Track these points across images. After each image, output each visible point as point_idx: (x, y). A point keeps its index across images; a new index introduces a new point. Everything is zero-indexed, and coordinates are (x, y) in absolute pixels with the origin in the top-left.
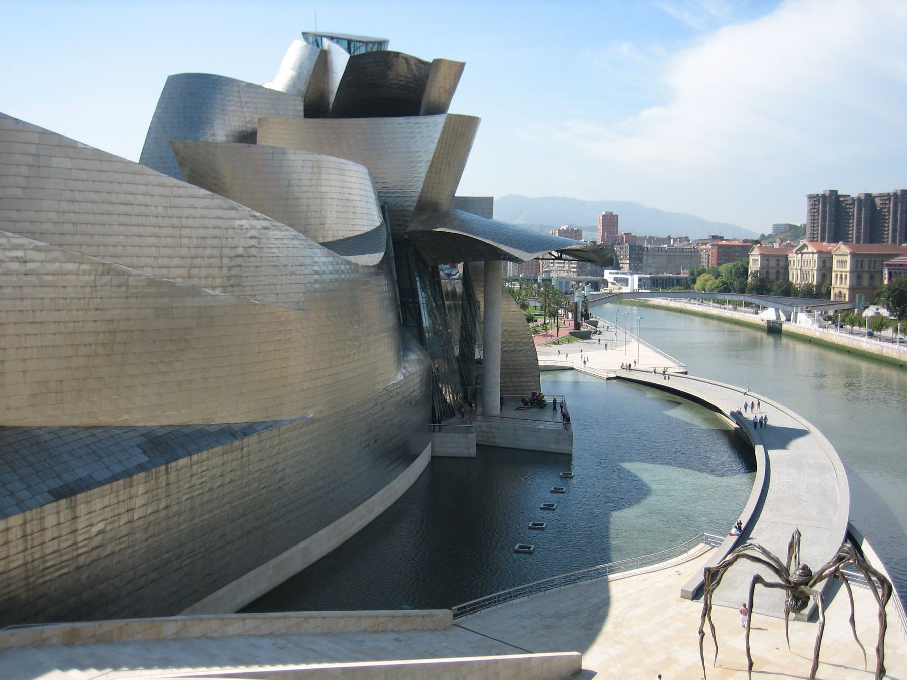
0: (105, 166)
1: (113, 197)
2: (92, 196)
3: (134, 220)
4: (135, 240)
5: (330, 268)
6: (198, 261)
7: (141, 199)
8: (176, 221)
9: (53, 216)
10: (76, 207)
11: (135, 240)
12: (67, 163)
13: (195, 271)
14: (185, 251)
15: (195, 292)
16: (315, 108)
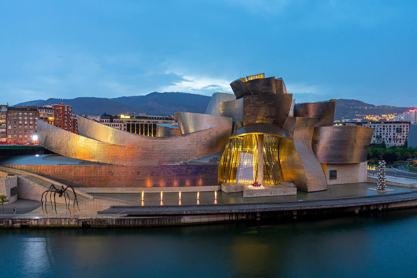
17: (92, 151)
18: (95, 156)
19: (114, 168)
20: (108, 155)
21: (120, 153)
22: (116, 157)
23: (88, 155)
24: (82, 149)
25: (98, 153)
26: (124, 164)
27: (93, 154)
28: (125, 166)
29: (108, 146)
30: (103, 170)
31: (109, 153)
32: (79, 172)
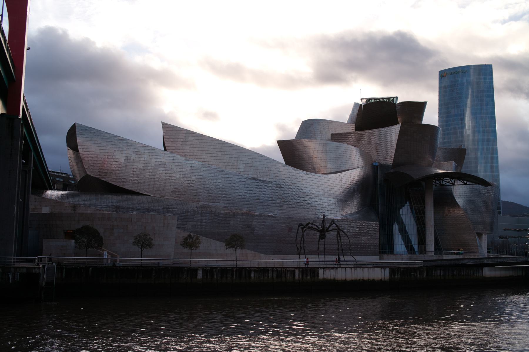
0: (203, 138)
1: (205, 146)
2: (200, 146)
3: (210, 152)
4: (210, 158)
5: (286, 171)
6: (229, 164)
7: (212, 147)
8: (223, 153)
9: (188, 151)
10: (194, 149)
11: (210, 158)
12: (193, 138)
13: (227, 167)
14: (225, 161)
15: (222, 171)
16: (358, 128)
17: (213, 187)
18: (219, 197)
19: (256, 219)
20: (245, 195)
21: (263, 194)
22: (258, 199)
23: (205, 194)
24: (194, 182)
25: (226, 192)
26: (271, 214)
27: (216, 192)
28: (272, 216)
29: (243, 180)
30: (238, 222)
31: (246, 193)
32: (199, 223)
